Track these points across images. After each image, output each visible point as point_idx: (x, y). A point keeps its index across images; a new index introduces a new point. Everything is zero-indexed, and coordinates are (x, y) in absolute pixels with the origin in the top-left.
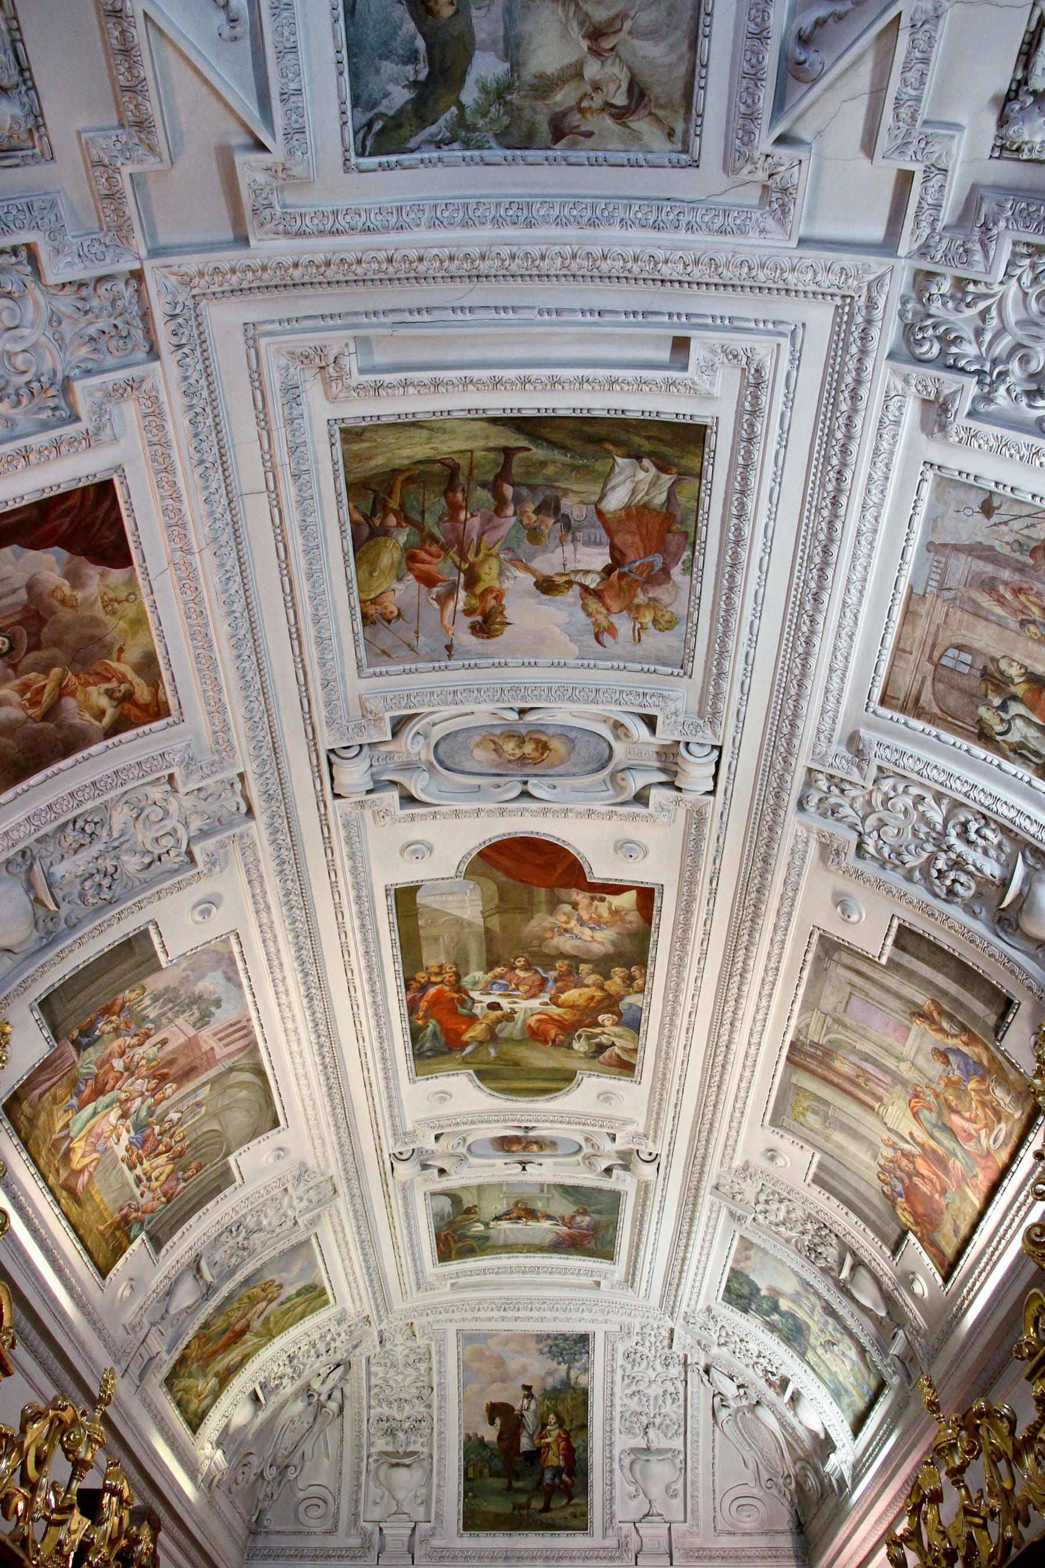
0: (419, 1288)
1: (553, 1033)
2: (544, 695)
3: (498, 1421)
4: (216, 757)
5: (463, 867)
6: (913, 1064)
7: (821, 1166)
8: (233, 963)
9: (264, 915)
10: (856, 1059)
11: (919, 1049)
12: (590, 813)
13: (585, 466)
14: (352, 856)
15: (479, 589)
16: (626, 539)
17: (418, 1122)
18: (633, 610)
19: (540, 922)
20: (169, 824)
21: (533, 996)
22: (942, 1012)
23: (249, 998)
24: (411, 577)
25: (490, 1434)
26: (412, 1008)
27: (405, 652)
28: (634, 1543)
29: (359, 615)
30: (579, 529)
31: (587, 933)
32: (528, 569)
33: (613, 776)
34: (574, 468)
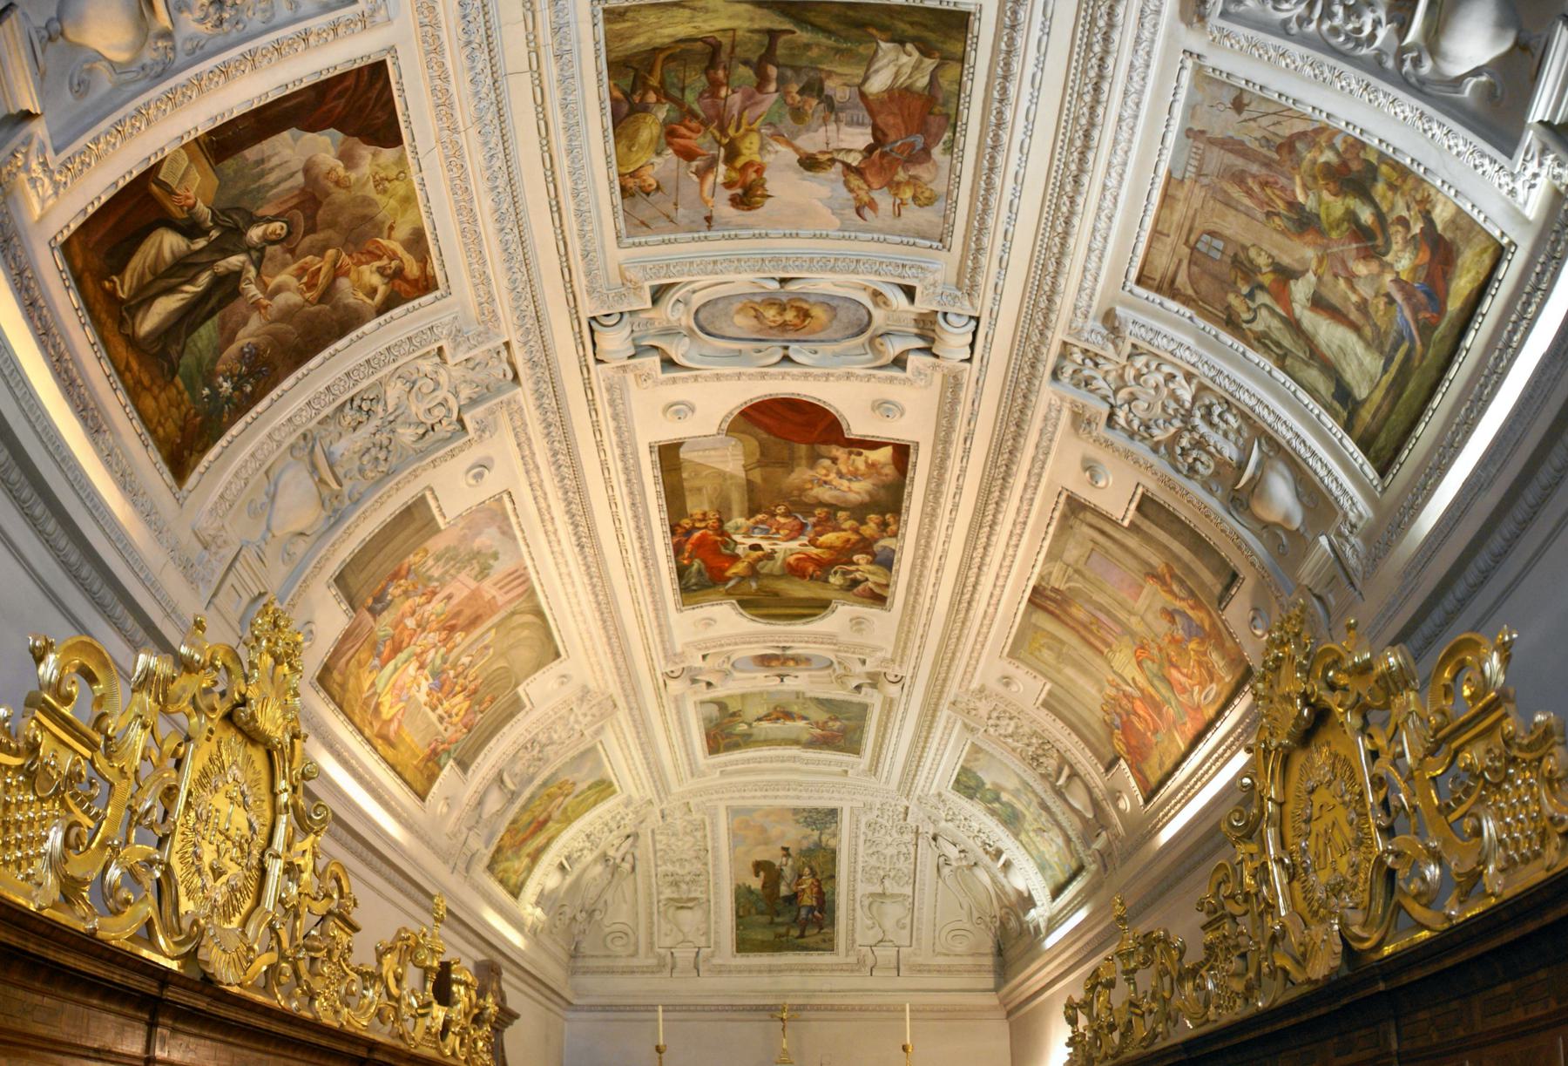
0: (692, 775)
1: (811, 570)
2: (806, 265)
3: (762, 874)
4: (481, 328)
5: (725, 426)
7: (1050, 693)
8: (506, 518)
9: (533, 474)
10: (1090, 608)
11: (1149, 606)
12: (849, 376)
13: (849, 50)
14: (615, 417)
15: (739, 163)
16: (887, 120)
17: (687, 644)
18: (894, 186)
19: (800, 475)
20: (440, 395)
21: (792, 539)
22: (1173, 576)
23: (524, 549)
24: (670, 151)
25: (756, 883)
26: (678, 550)
27: (664, 223)
28: (870, 961)
29: (618, 188)
30: (842, 109)
31: (845, 483)
32: (789, 144)
33: (871, 341)
34: (838, 51)
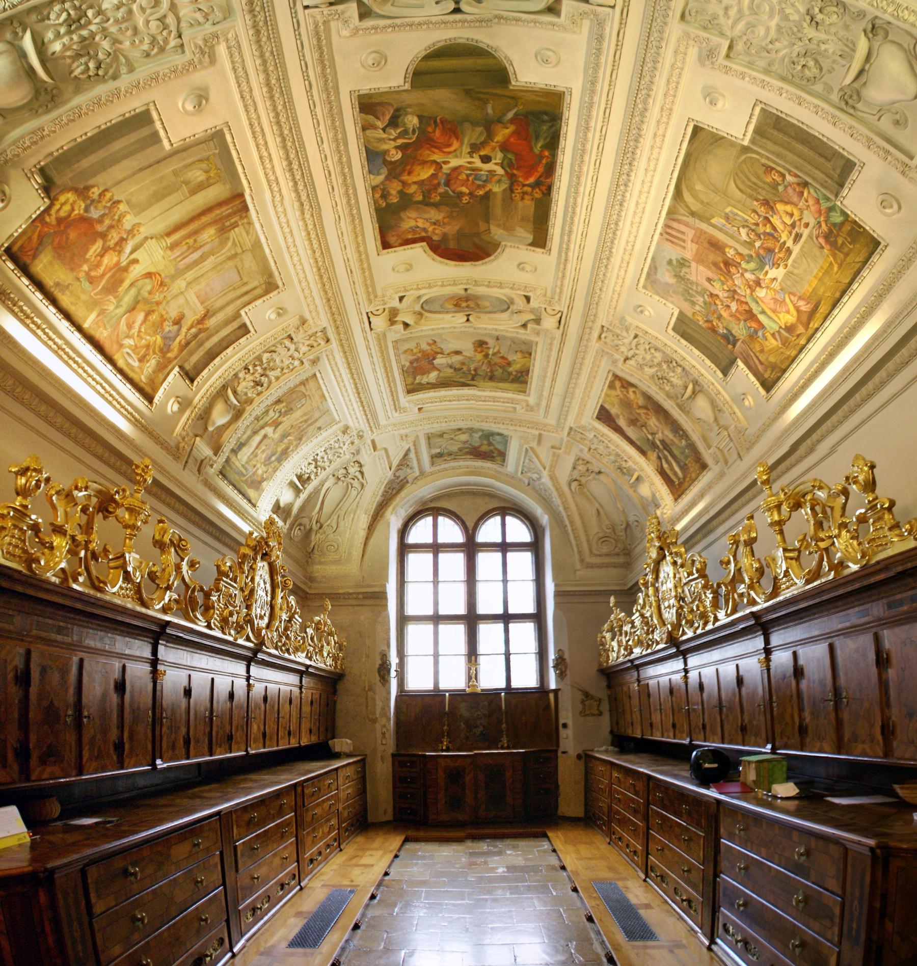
6: (182, 293)
8: (648, 274)
10: (206, 249)
26: (550, 169)
